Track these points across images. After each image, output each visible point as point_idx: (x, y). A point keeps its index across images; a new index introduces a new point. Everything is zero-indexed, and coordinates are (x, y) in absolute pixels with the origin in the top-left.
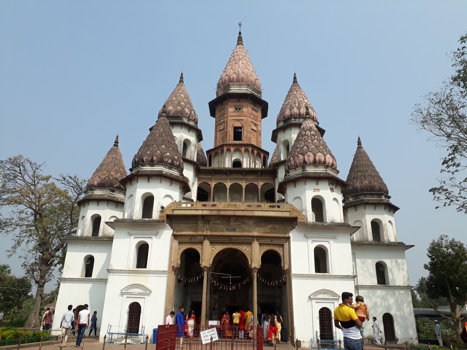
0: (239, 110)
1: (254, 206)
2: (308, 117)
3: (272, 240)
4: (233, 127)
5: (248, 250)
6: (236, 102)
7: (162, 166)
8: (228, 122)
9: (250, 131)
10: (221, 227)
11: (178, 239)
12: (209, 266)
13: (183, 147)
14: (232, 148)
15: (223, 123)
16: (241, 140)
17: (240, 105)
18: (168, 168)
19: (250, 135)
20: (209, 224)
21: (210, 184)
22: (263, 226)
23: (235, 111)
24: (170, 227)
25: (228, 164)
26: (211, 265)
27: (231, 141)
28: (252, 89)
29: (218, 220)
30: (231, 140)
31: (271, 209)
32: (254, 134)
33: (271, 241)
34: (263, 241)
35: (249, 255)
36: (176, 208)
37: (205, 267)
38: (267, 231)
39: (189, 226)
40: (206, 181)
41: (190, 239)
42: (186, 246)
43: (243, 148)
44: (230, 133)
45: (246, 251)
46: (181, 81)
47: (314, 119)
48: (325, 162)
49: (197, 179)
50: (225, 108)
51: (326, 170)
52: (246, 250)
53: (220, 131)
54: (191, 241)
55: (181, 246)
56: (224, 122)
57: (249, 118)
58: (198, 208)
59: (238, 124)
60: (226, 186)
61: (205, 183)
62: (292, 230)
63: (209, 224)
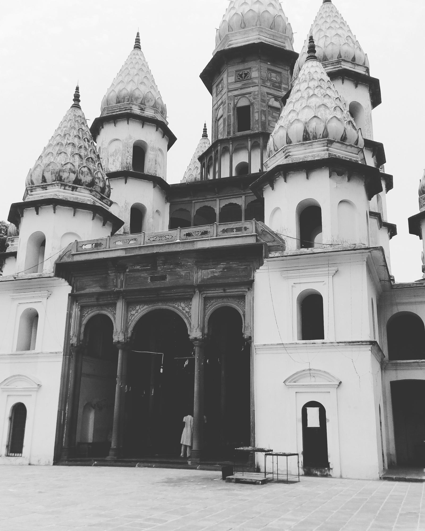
0: (245, 77)
1: (196, 233)
2: (313, 56)
3: (224, 290)
4: (236, 110)
5: (187, 309)
6: (238, 63)
7: (57, 187)
8: (227, 101)
9: (264, 111)
10: (142, 275)
11: (79, 302)
12: (123, 341)
13: (132, 154)
14: (231, 145)
15: (221, 106)
16: (250, 129)
17: (246, 67)
18: (71, 189)
19: (266, 118)
20: (124, 273)
21: (189, 210)
22: (210, 267)
23: (239, 80)
24: (67, 284)
25: (225, 174)
26: (128, 340)
27: (232, 134)
28: (268, 36)
29: (138, 264)
30: (232, 132)
31: (226, 235)
32: (274, 114)
33: (222, 291)
34: (211, 293)
35: (190, 319)
36: (77, 251)
37: (119, 342)
38: (216, 274)
39: (95, 279)
40: (183, 206)
41: (98, 299)
42: (92, 312)
43: (249, 143)
44: (230, 120)
45: (184, 311)
46: (137, 46)
47: (357, 62)
48: (326, 135)
49: (168, 205)
50: (222, 79)
51: (328, 150)
52: (184, 310)
53: (218, 120)
54: (99, 302)
55: (86, 312)
56: (222, 103)
57: (262, 87)
58: (109, 248)
59: (243, 102)
60: (214, 210)
61: (181, 210)
62: (258, 269)
63: (124, 273)
